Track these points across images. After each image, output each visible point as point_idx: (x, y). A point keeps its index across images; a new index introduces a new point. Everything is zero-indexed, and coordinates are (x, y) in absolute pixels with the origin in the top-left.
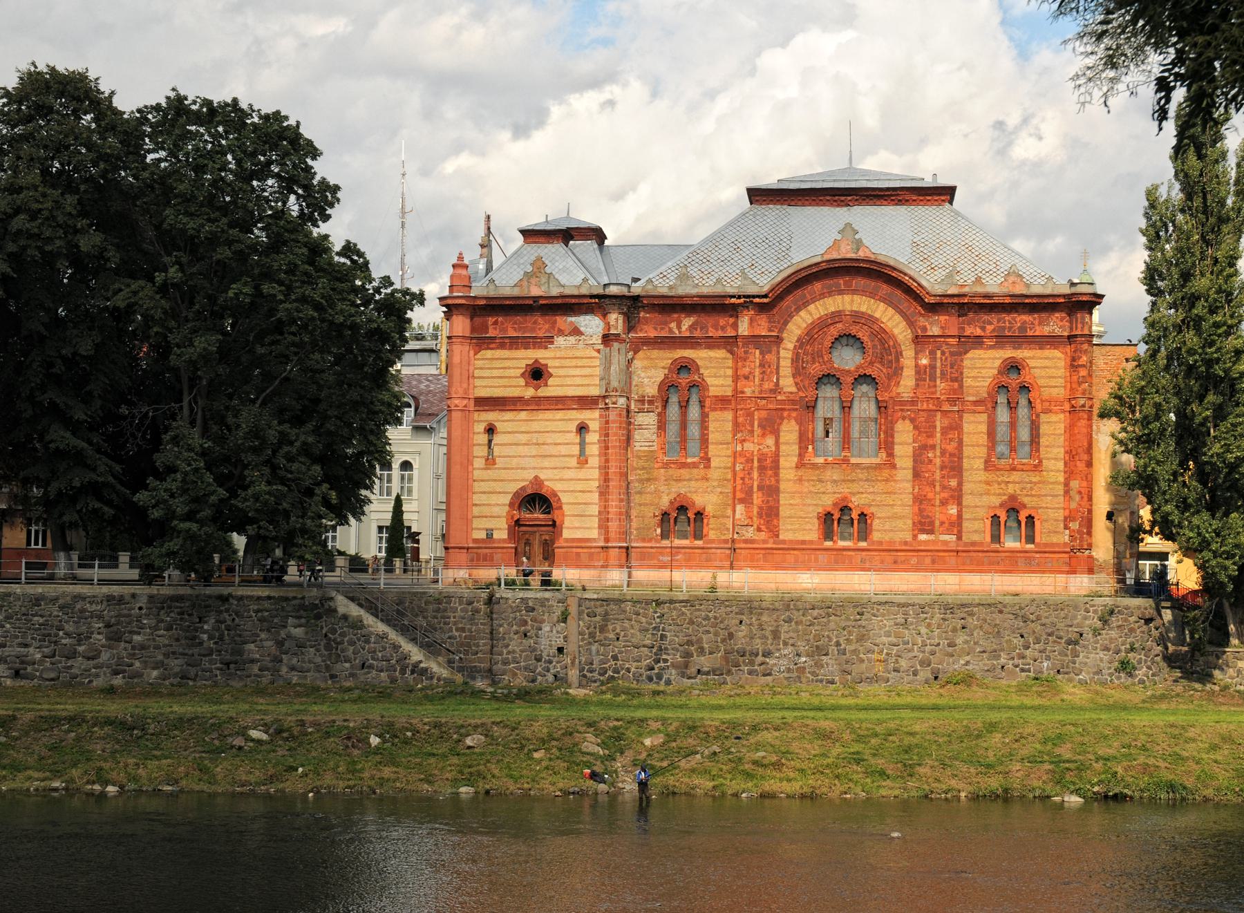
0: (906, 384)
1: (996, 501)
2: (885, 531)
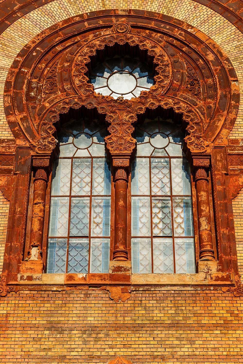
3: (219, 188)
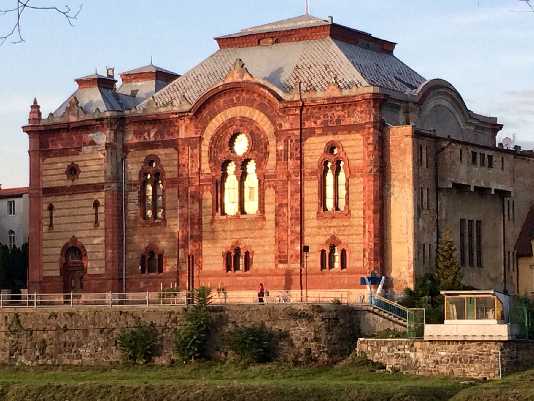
1: (323, 240)
2: (260, 262)
3: (262, 187)
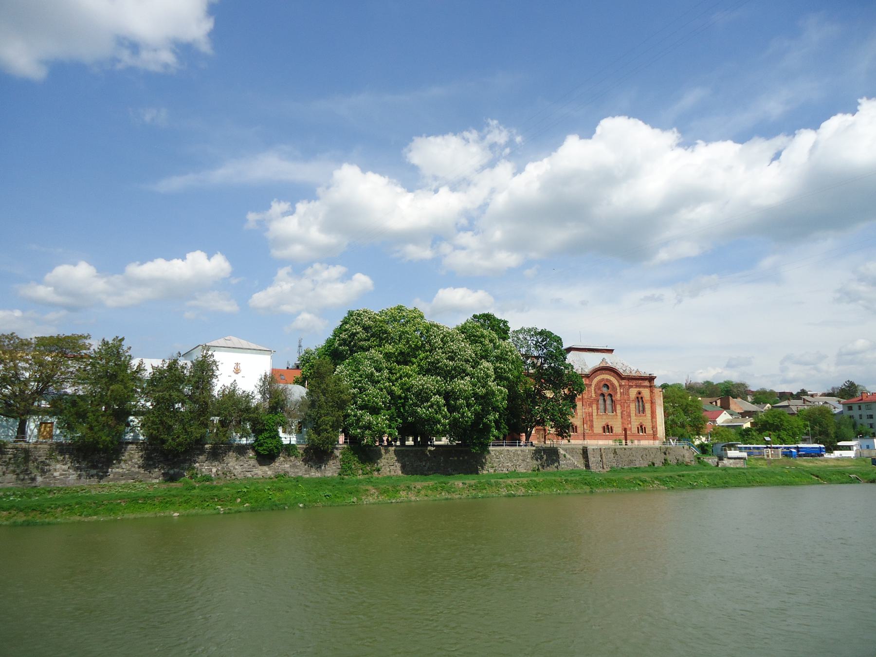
0: (618, 396)
